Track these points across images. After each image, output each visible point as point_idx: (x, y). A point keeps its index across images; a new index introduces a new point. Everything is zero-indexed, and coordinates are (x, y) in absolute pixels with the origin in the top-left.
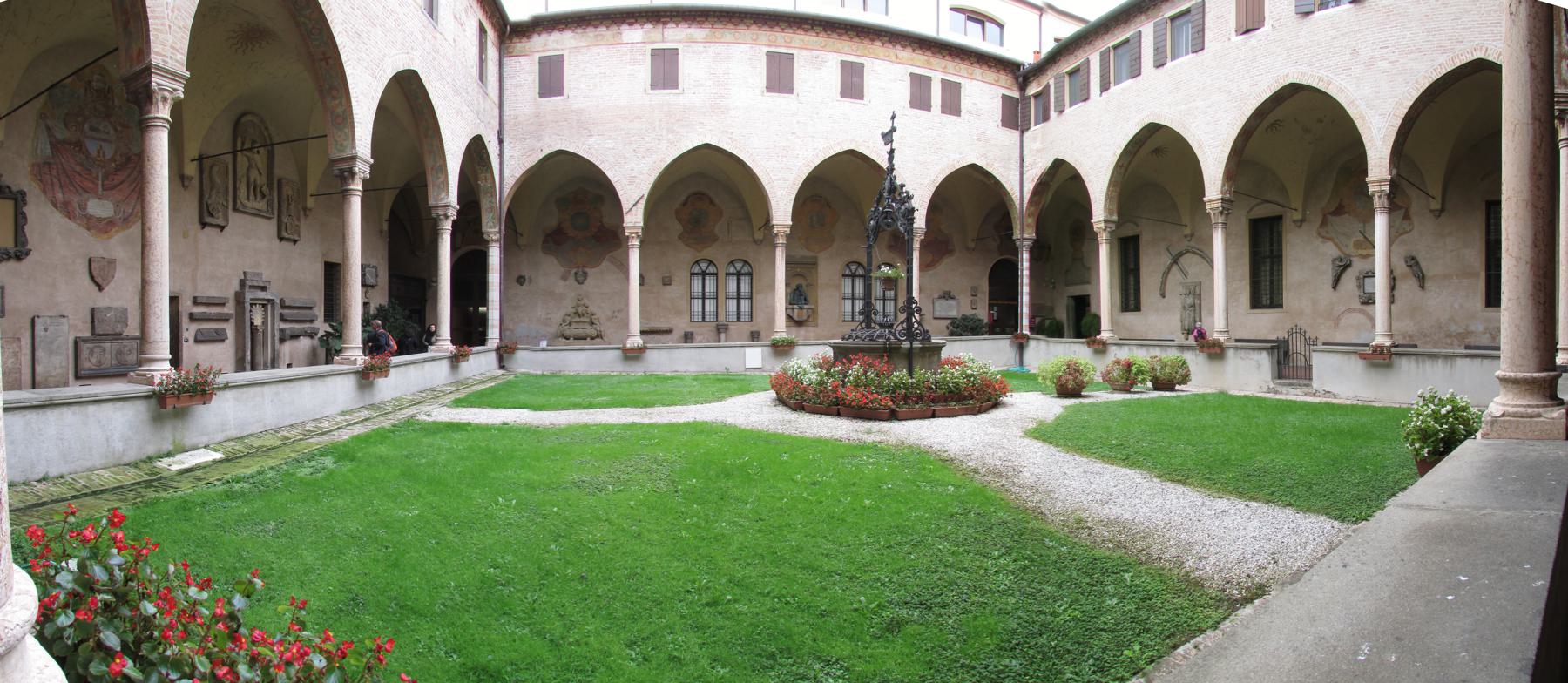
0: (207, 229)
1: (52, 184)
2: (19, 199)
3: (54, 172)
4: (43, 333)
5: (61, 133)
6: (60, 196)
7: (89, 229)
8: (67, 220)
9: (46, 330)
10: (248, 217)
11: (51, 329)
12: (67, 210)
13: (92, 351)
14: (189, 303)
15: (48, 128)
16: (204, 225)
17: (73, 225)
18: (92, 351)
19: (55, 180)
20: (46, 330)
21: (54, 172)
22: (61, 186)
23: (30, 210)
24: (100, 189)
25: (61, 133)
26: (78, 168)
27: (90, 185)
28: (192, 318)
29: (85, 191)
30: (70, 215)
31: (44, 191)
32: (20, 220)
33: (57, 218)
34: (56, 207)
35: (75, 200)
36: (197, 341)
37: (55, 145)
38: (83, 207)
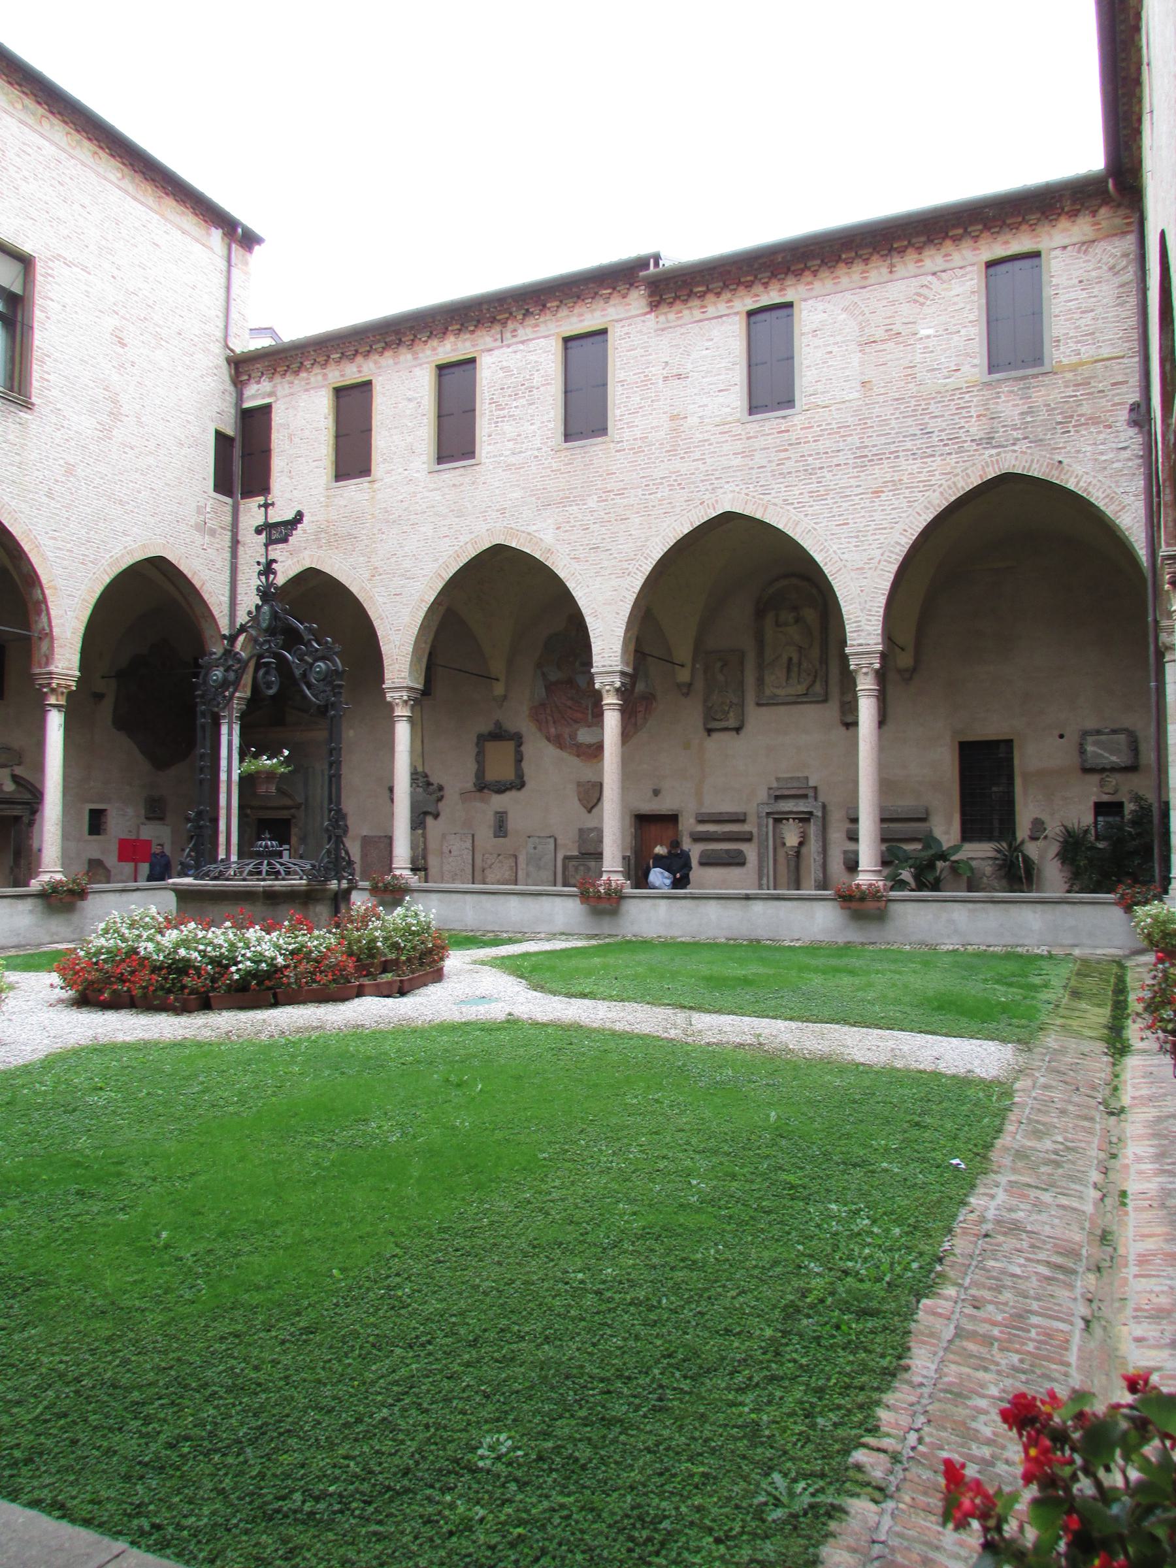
0: (715, 736)
1: (547, 722)
2: (518, 739)
3: (548, 711)
4: (532, 851)
5: (555, 675)
6: (553, 730)
7: (578, 756)
8: (558, 750)
9: (535, 848)
10: (782, 708)
11: (540, 847)
12: (558, 742)
13: (576, 869)
14: (692, 821)
15: (543, 674)
16: (709, 731)
17: (565, 755)
18: (576, 869)
19: (549, 718)
20: (535, 848)
21: (548, 711)
22: (554, 722)
23: (528, 749)
24: (590, 717)
25: (555, 675)
26: (569, 703)
27: (579, 715)
28: (697, 838)
29: (576, 721)
30: (561, 746)
31: (540, 730)
32: (519, 759)
33: (551, 751)
34: (549, 740)
35: (566, 731)
36: (702, 864)
37: (550, 687)
38: (573, 736)
